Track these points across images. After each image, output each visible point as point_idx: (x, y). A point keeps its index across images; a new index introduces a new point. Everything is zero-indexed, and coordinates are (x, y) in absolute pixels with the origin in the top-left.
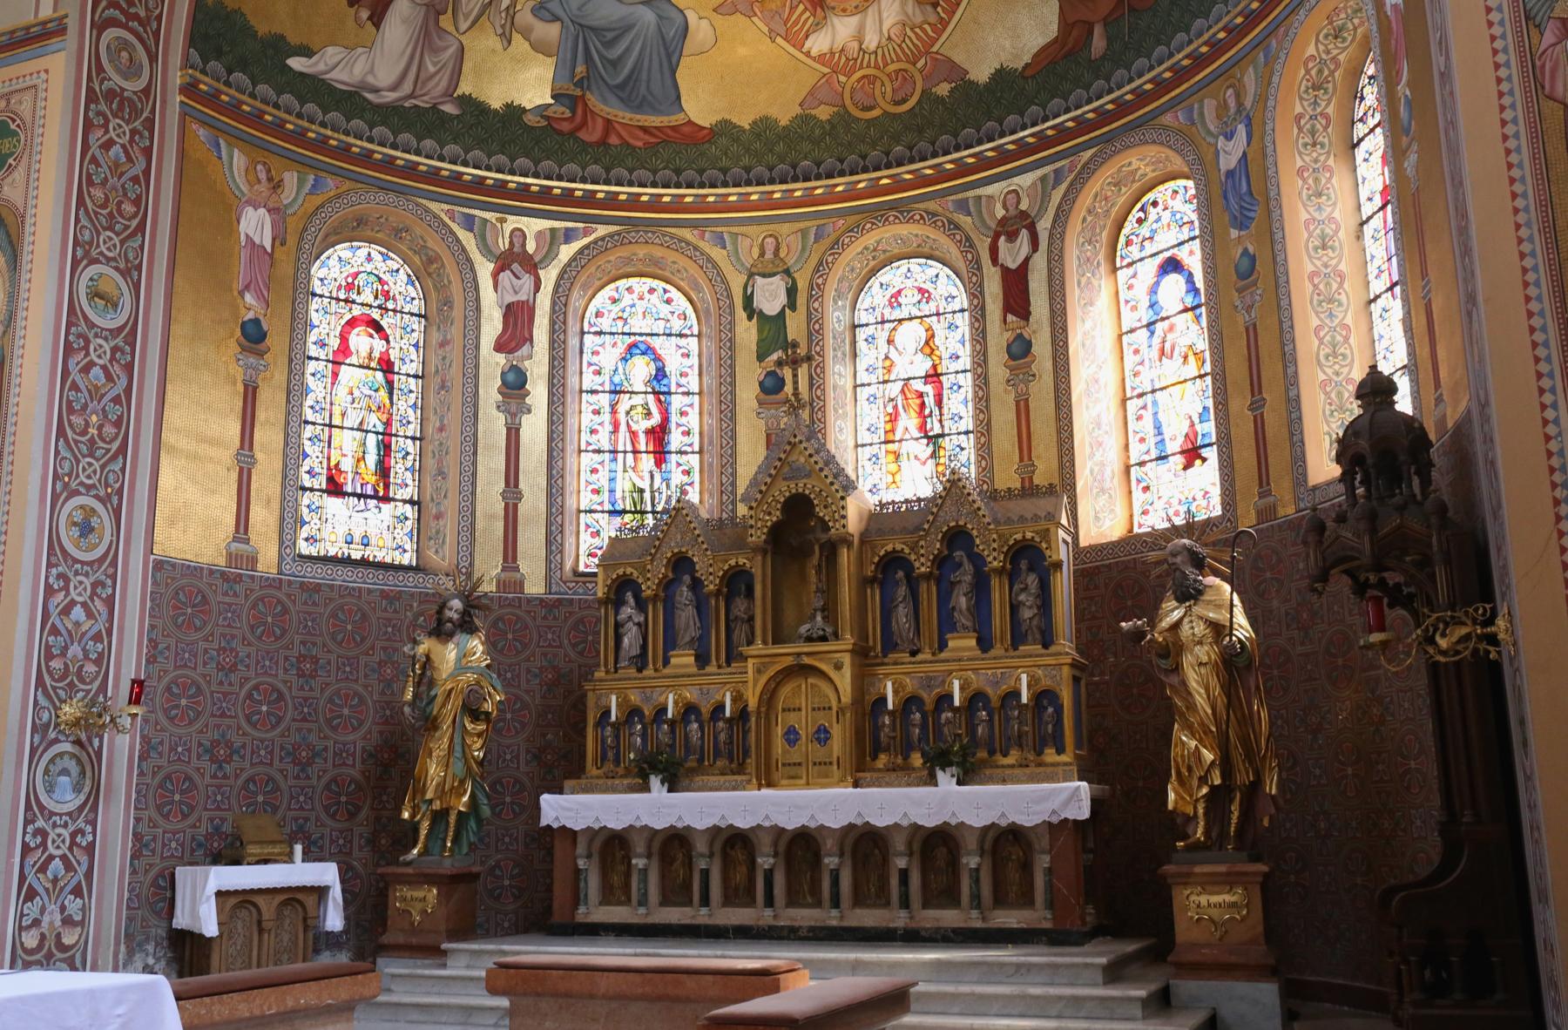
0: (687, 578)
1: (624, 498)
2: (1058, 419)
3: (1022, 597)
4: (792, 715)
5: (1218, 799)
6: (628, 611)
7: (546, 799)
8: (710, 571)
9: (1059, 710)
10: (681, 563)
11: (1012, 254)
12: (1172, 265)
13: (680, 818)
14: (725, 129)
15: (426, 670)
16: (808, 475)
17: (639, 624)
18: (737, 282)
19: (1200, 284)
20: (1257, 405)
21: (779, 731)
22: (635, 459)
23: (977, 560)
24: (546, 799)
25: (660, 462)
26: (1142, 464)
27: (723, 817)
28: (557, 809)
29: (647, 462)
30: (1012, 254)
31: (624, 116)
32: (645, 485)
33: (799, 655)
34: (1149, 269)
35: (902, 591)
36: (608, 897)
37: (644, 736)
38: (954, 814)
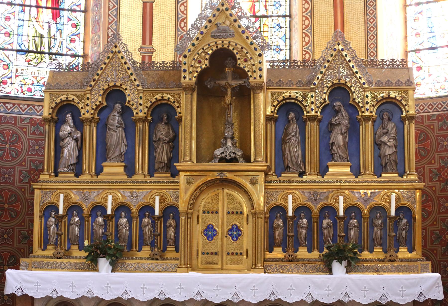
0: (118, 106)
1: (28, 41)
2: (366, 14)
3: (385, 139)
4: (210, 216)
6: (67, 129)
7: (10, 273)
8: (140, 103)
9: (411, 219)
10: (115, 94)
13: (125, 292)
16: (232, 36)
17: (76, 140)
21: (201, 228)
22: (38, 12)
23: (353, 108)
24: (10, 273)
25: (55, 16)
26: (417, 51)
27: (162, 292)
29: (47, 15)
32: (44, 32)
33: (222, 171)
35: (294, 127)
37: (81, 225)
38: (346, 294)
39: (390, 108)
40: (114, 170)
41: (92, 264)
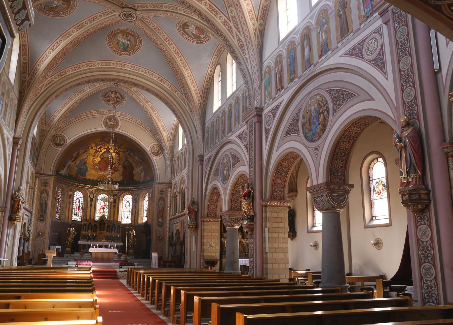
5: (132, 244)
8: (93, 224)
10: (90, 223)
11: (115, 197)
12: (128, 202)
14: (89, 179)
15: (69, 230)
18: (89, 194)
19: (131, 205)
20: (135, 216)
28: (80, 242)
30: (115, 197)
31: (81, 177)
34: (126, 201)
36: (83, 249)
39: (119, 226)
40: (89, 231)
41: (88, 241)
